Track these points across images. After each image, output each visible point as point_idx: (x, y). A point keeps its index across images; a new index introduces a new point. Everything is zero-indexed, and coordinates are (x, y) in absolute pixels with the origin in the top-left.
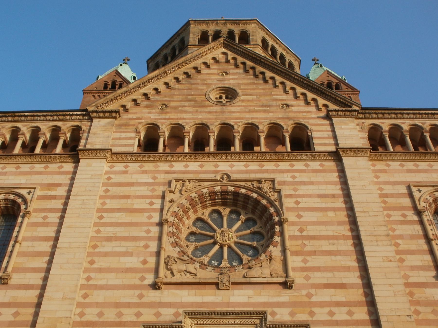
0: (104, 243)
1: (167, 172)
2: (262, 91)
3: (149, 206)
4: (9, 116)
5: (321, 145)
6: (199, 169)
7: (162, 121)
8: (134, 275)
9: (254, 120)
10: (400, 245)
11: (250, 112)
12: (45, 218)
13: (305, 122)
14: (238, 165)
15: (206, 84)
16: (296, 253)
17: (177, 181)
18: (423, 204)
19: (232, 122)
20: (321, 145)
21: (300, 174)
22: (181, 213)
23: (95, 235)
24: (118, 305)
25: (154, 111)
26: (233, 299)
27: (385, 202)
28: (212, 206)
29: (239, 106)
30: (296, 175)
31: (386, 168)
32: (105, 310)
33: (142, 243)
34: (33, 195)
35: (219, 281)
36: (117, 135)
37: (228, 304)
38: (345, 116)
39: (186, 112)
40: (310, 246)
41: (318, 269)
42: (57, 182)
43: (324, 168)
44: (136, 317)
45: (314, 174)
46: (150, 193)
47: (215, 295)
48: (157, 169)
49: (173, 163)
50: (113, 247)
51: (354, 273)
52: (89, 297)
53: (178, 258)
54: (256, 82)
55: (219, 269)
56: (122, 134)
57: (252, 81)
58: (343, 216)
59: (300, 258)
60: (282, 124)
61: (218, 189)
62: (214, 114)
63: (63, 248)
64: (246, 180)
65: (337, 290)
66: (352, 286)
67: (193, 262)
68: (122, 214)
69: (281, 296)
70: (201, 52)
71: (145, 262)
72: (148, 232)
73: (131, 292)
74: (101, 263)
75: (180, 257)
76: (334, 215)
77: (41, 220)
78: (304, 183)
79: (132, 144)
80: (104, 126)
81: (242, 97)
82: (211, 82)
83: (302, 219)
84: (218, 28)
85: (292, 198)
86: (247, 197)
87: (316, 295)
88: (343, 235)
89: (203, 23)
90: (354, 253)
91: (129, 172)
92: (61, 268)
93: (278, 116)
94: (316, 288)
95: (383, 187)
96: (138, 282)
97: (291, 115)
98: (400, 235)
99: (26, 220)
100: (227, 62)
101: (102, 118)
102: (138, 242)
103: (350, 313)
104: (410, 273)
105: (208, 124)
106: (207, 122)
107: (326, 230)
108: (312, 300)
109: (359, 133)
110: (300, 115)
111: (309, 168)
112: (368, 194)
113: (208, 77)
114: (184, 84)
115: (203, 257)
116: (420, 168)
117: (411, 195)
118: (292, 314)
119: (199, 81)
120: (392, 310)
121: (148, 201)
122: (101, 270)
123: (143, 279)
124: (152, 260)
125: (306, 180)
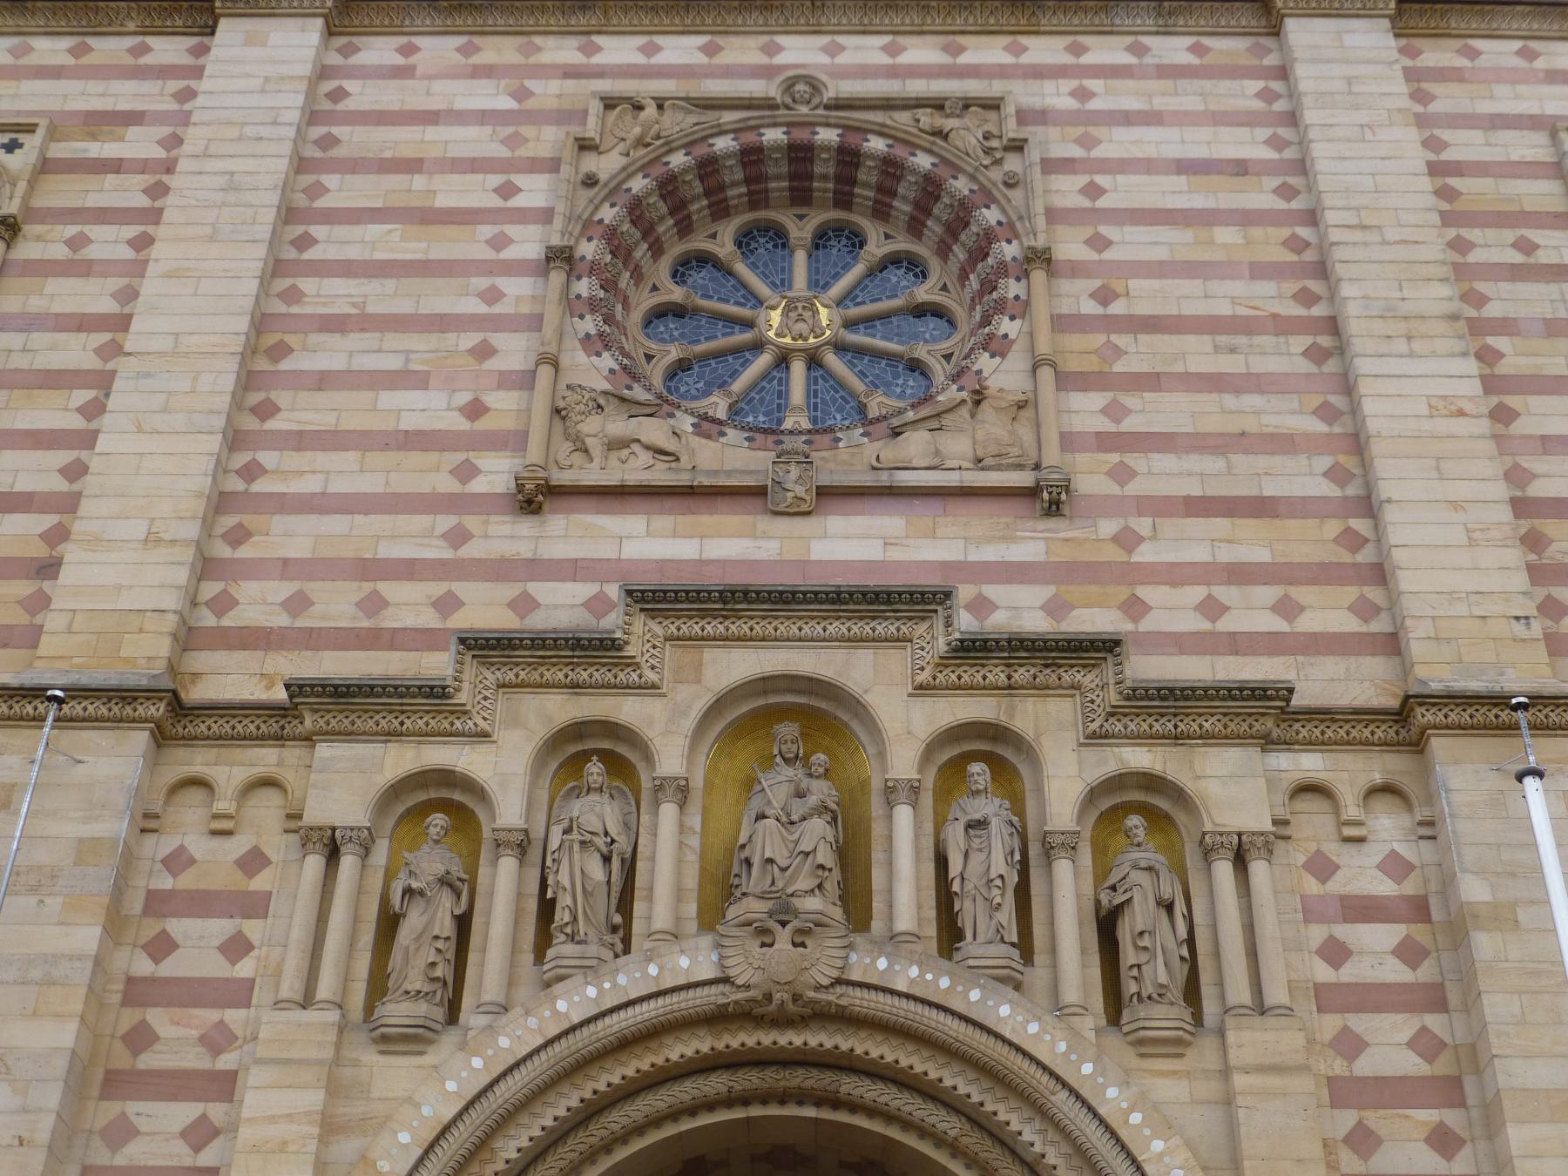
0: (315, 339)
1: (570, 73)
6: (701, 59)
8: (433, 457)
10: (1502, 355)
12: (76, 243)
14: (857, 48)
17: (609, 103)
21: (1111, 82)
24: (370, 569)
30: (1094, 84)
31: (1462, 62)
32: (314, 588)
33: (469, 340)
35: (769, 483)
40: (1139, 354)
44: (437, 615)
45: (1167, 84)
46: (504, 152)
47: (753, 535)
48: (533, 60)
49: (597, 39)
50: (351, 354)
51: (1309, 458)
52: (253, 539)
53: (605, 393)
55: (771, 438)
61: (774, 136)
63: (149, 353)
65: (1238, 521)
67: (666, 408)
68: (390, 231)
69: (1013, 540)
71: (475, 410)
72: (492, 296)
73: (421, 521)
75: (615, 392)
76: (1241, 241)
77: (60, 252)
83: (1108, 255)
85: (1074, 172)
87: (1154, 538)
88: (1275, 316)
91: (419, 72)
92: (140, 430)
96: (448, 484)
98: (1505, 319)
102: (451, 336)
103: (1286, 608)
107: (1206, 297)
108: (1136, 558)
112: (1383, 158)
115: (713, 399)
118: (1054, 608)
120: (1456, 596)
121: (495, 180)
125: (1133, 104)
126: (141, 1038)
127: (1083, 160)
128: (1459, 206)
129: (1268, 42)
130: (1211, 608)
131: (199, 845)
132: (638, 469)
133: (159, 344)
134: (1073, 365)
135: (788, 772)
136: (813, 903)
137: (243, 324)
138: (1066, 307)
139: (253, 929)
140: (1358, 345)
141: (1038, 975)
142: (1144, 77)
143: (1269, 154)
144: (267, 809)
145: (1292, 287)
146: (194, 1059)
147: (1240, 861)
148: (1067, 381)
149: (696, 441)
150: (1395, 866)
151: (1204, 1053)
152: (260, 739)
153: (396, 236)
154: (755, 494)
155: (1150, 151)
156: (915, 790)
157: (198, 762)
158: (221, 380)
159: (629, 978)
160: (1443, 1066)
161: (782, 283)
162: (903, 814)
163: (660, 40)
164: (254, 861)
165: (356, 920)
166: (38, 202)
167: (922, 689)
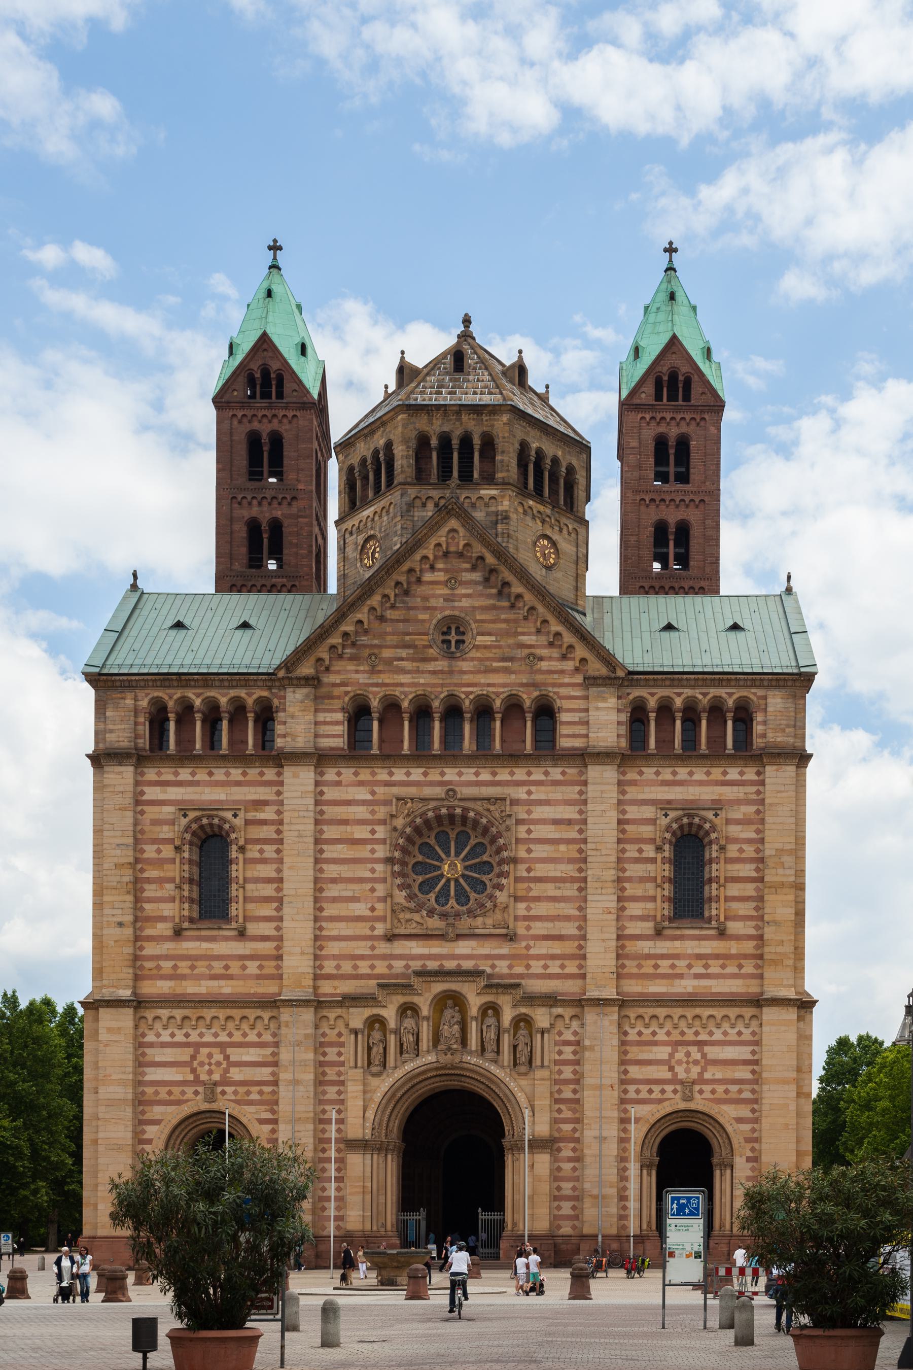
0: (330, 885)
1: (387, 784)
2: (504, 626)
3: (369, 836)
7: (375, 689)
8: (364, 924)
9: (491, 689)
13: (555, 693)
15: (428, 608)
17: (398, 799)
19: (463, 692)
25: (362, 668)
26: (458, 951)
28: (439, 826)
29: (472, 659)
30: (533, 788)
31: (638, 778)
32: (342, 963)
36: (321, 717)
38: (605, 685)
40: (537, 889)
42: (262, 798)
43: (567, 777)
48: (375, 779)
56: (327, 715)
57: (492, 602)
60: (525, 696)
62: (440, 676)
64: (475, 799)
69: (501, 948)
71: (373, 909)
73: (363, 943)
77: (257, 855)
80: (302, 702)
81: (479, 638)
82: (435, 604)
83: (531, 855)
84: (446, 428)
89: (422, 410)
93: (520, 681)
94: (535, 940)
96: (369, 933)
97: (539, 678)
101: (298, 686)
103: (562, 967)
105: (433, 697)
106: (431, 692)
111: (549, 778)
113: (431, 592)
116: (678, 777)
118: (510, 967)
119: (419, 600)
121: (369, 828)
122: (332, 919)
125: (543, 797)
126: (324, 1074)
127: (528, 820)
128: (626, 836)
129: (583, 770)
130: (546, 967)
131: (328, 1031)
132: (412, 929)
133: (293, 892)
134: (520, 894)
135: (451, 1011)
136: (455, 1046)
137: (312, 885)
138: (519, 874)
139: (342, 1050)
140: (589, 891)
141: (500, 1057)
143: (577, 816)
144: (340, 1023)
145: (577, 866)
146: (335, 1078)
147: (543, 1033)
148: (517, 899)
149: (427, 919)
150: (575, 1033)
151: (531, 1075)
152: (337, 1007)
153: (345, 849)
154: (442, 937)
155: (545, 816)
156: (476, 1019)
157: (325, 1012)
158: (309, 904)
159: (419, 1062)
160: (577, 1077)
161: (448, 854)
162: (474, 1023)
163: (411, 770)
164: (340, 1035)
165: (363, 1047)
166: (249, 837)
167: (478, 994)
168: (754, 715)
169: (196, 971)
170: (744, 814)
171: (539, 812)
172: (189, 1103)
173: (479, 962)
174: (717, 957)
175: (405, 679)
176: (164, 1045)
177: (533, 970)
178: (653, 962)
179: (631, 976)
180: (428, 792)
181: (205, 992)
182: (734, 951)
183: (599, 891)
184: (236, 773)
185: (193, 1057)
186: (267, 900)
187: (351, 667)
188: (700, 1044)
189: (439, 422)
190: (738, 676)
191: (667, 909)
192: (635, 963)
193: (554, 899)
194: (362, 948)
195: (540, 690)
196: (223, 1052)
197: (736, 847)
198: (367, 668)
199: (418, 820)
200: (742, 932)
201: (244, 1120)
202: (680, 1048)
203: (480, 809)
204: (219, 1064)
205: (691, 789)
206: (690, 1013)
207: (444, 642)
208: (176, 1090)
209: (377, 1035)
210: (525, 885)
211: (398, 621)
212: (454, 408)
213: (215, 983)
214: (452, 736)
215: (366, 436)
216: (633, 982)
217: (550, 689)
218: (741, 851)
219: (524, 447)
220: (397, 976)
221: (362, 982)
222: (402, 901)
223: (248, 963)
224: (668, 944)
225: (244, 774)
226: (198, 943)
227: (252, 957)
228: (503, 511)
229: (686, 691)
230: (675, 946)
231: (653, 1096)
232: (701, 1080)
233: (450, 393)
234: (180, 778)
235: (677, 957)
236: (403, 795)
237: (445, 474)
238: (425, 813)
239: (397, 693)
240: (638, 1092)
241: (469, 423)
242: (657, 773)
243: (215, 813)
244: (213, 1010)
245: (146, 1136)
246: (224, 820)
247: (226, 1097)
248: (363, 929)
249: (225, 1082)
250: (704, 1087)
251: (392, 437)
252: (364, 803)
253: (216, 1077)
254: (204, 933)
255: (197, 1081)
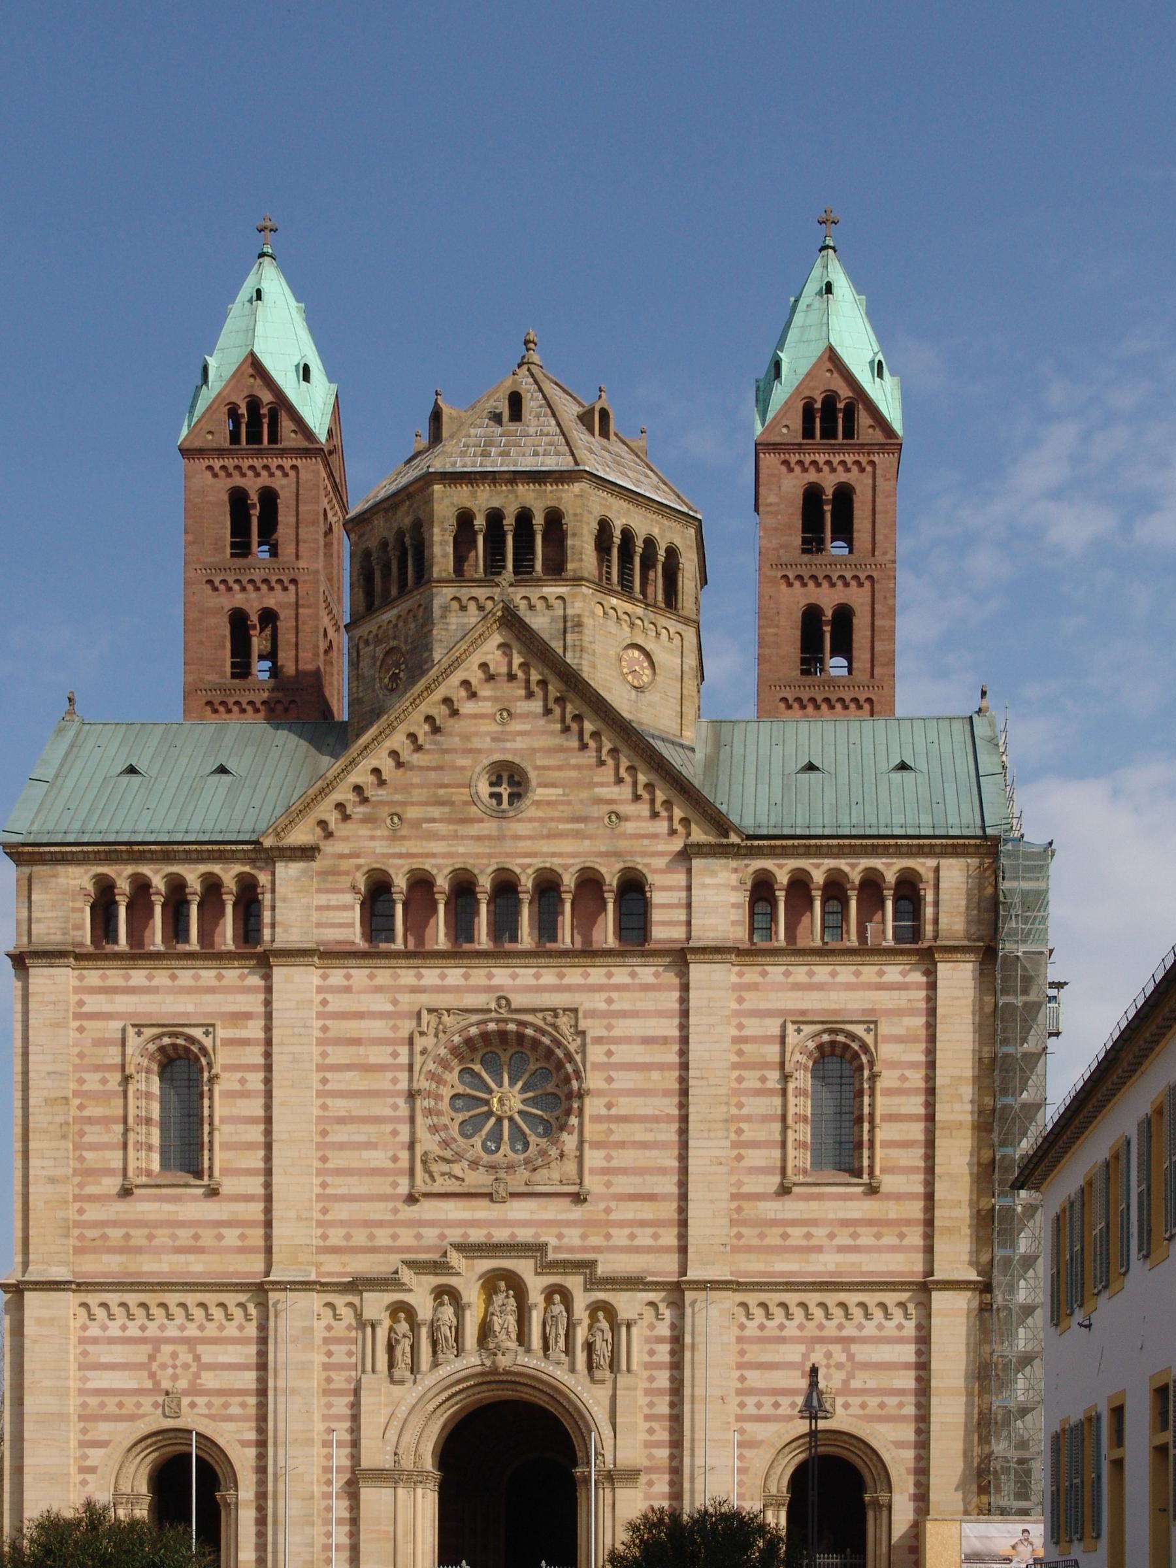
0: (336, 1127)
1: (414, 990)
2: (574, 774)
3: (390, 1060)
4: (121, 851)
5: (664, 923)
11: (551, 836)
13: (645, 865)
15: (470, 751)
16: (597, 1145)
17: (430, 1011)
18: (798, 1057)
19: (520, 865)
20: (664, 923)
22: (440, 1070)
23: (321, 1113)
24: (368, 1224)
25: (378, 833)
27: (740, 1053)
28: (486, 1046)
29: (531, 820)
30: (615, 995)
31: (759, 979)
32: (353, 1231)
34: (214, 1038)
36: (322, 899)
37: (506, 1223)
39: (435, 836)
40: (620, 1132)
41: (623, 1171)
42: (243, 1010)
45: (643, 994)
47: (489, 1210)
48: (397, 983)
54: (566, 744)
56: (331, 896)
58: (671, 1080)
59: (601, 1153)
60: (603, 870)
61: (492, 1026)
62: (487, 843)
64: (533, 1011)
66: (664, 1197)
69: (570, 1211)
70: (457, 654)
71: (395, 1159)
73: (382, 1205)
74: (338, 1160)
77: (237, 1087)
78: (623, 1014)
79: (350, 921)
80: (298, 879)
81: (540, 791)
82: (479, 746)
83: (614, 1086)
86: (535, 1043)
90: (677, 1146)
95: (745, 1021)
96: (389, 1190)
97: (623, 844)
99: (217, 1089)
100: (511, 677)
102: (383, 1126)
103: (655, 1236)
104: (745, 1179)
105: (476, 872)
106: (474, 865)
109: (733, 894)
110: (638, 845)
111: (637, 981)
113: (473, 729)
114: (428, 750)
116: (816, 979)
117: (783, 1039)
118: (584, 1237)
119: (457, 739)
121: (390, 1049)
122: (339, 1172)
123: (395, 1185)
124: (404, 1155)
125: (627, 1006)
127: (607, 1037)
130: (632, 1236)
142: (634, 991)
147: (629, 1326)
154: (489, 1196)
168: (922, 892)
169: (155, 1242)
170: (908, 1029)
171: (623, 1027)
172: (147, 1419)
173: (539, 1230)
174: (870, 1223)
175: (438, 847)
176: (112, 1341)
177: (613, 1242)
178: (780, 1230)
179: (749, 1249)
180: (470, 1001)
181: (167, 1270)
182: (892, 1215)
183: (706, 1134)
184: (208, 976)
185: (152, 1358)
186: (250, 1146)
187: (364, 831)
188: (846, 1341)
189: (486, 495)
190: (899, 841)
191: (799, 1158)
192: (757, 1231)
193: (644, 1145)
194: (379, 1211)
195: (625, 862)
196: (192, 1350)
197: (897, 1073)
198: (386, 833)
199: (457, 1039)
200: (904, 1189)
201: (221, 1442)
202: (817, 1346)
203: (541, 1023)
204: (186, 1366)
205: (833, 995)
206: (831, 1298)
207: (492, 795)
208: (129, 1401)
209: (403, 1327)
210: (604, 1126)
211: (429, 768)
212: (507, 476)
213: (182, 1258)
214: (504, 927)
215: (386, 510)
216: (752, 1257)
217: (638, 859)
218: (903, 1078)
219: (604, 526)
220: (428, 1249)
221: (381, 1257)
222: (437, 1150)
223: (225, 1231)
224: (802, 1205)
225: (220, 977)
226: (156, 1205)
227: (229, 1224)
228: (574, 616)
229: (826, 861)
230: (812, 1209)
231: (780, 1411)
232: (846, 1390)
233: (501, 454)
234: (132, 983)
235: (814, 1223)
236: (434, 1005)
237: (494, 563)
238: (466, 1028)
239: (427, 867)
240: (759, 1405)
241: (529, 496)
242: (787, 974)
243: (180, 1029)
244: (178, 1295)
245: (88, 1463)
246: (191, 1039)
247: (196, 1410)
248: (381, 1186)
249: (195, 1390)
250: (851, 1400)
251: (421, 515)
252: (383, 1015)
253: (183, 1384)
254: (165, 1191)
255: (156, 1389)
